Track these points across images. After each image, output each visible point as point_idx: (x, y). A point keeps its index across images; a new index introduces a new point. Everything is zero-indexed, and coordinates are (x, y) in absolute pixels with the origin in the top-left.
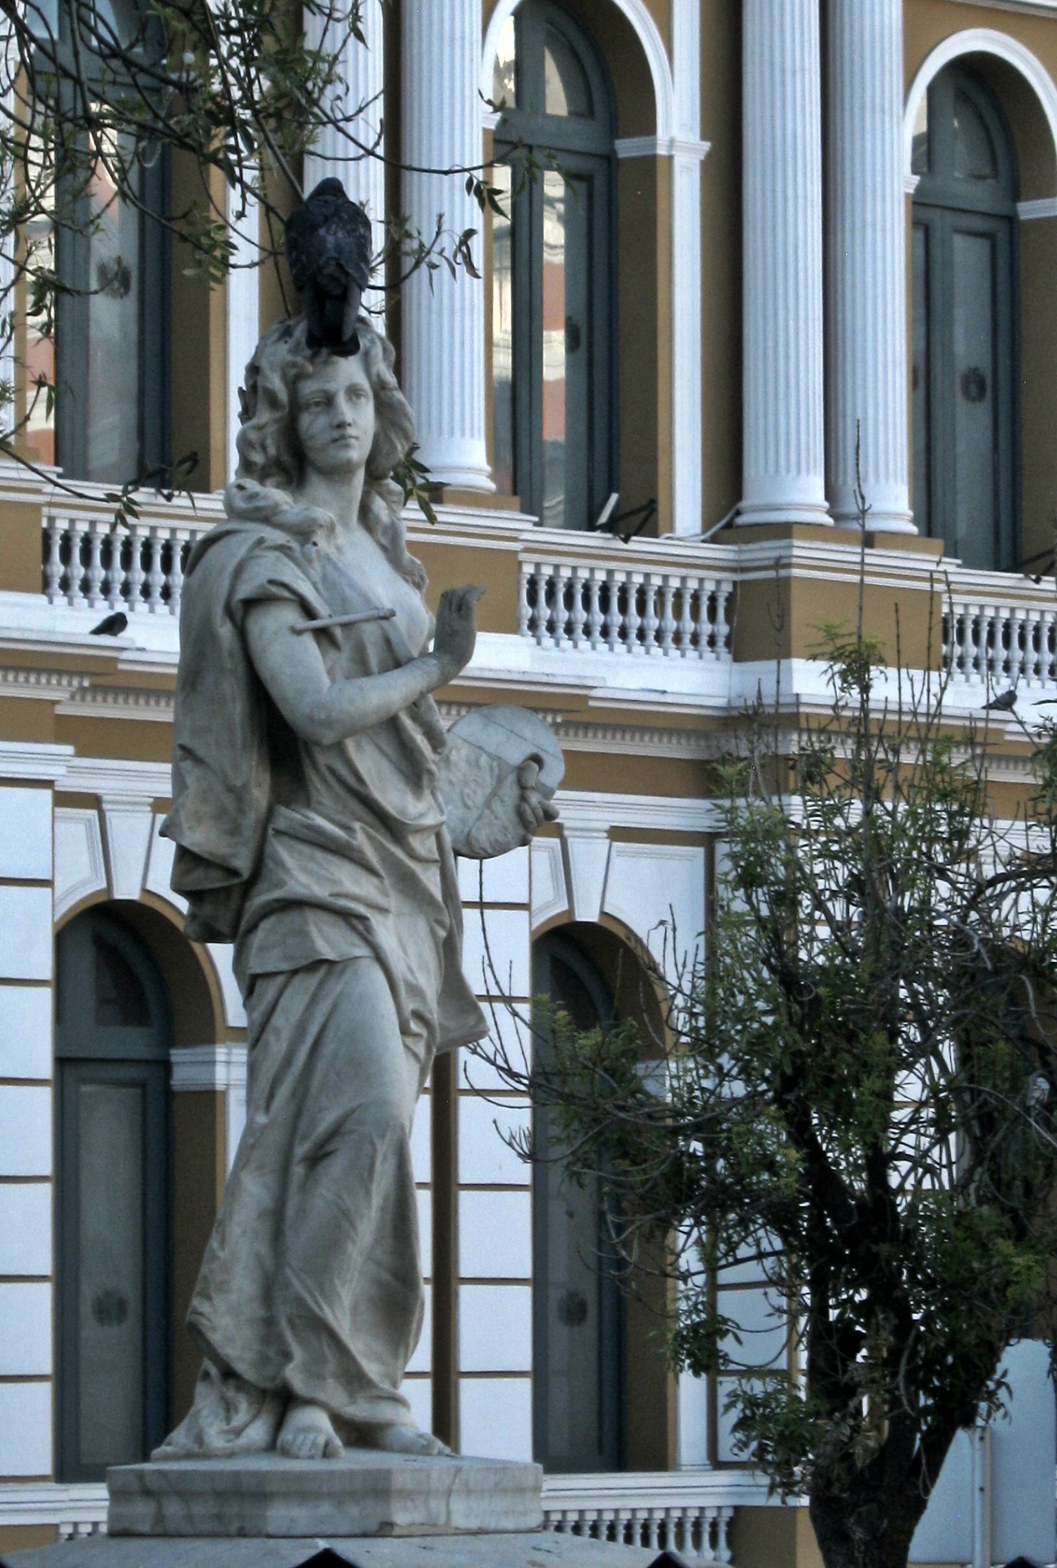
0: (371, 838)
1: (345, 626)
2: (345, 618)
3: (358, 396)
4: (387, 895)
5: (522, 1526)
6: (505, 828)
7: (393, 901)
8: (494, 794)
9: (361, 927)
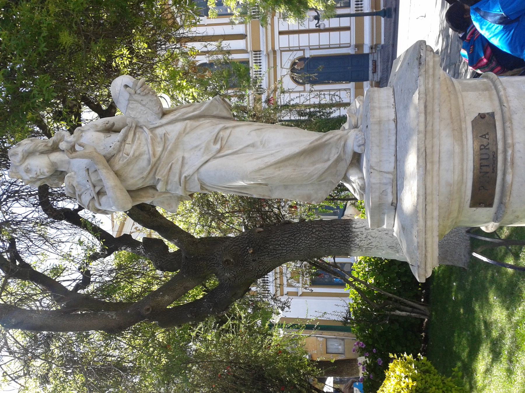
0: (160, 171)
1: (94, 186)
2: (92, 188)
3: (28, 168)
4: (178, 159)
5: (395, 132)
6: (150, 100)
7: (179, 154)
8: (140, 103)
9: (188, 178)
